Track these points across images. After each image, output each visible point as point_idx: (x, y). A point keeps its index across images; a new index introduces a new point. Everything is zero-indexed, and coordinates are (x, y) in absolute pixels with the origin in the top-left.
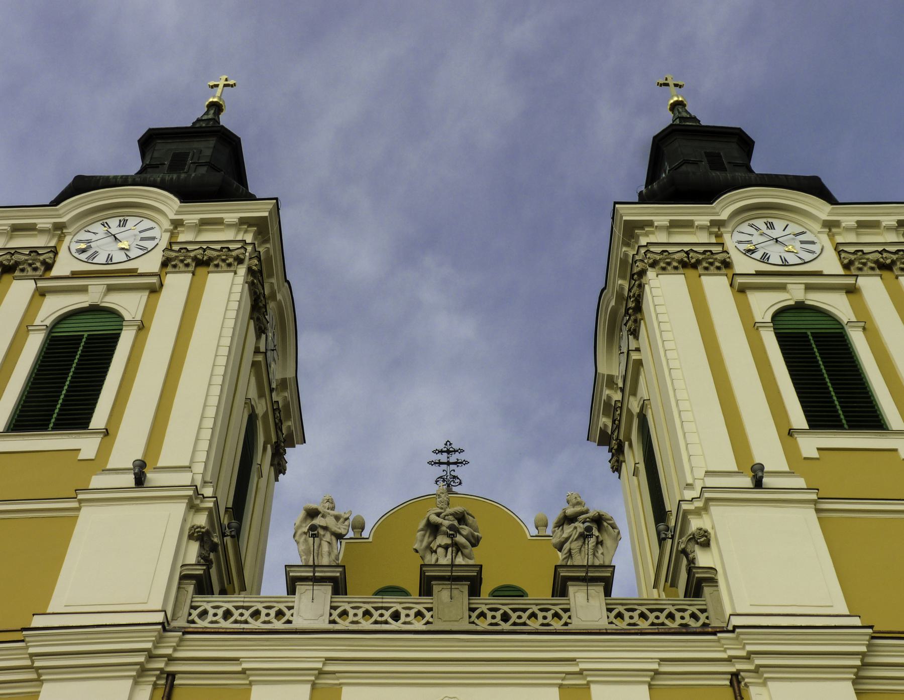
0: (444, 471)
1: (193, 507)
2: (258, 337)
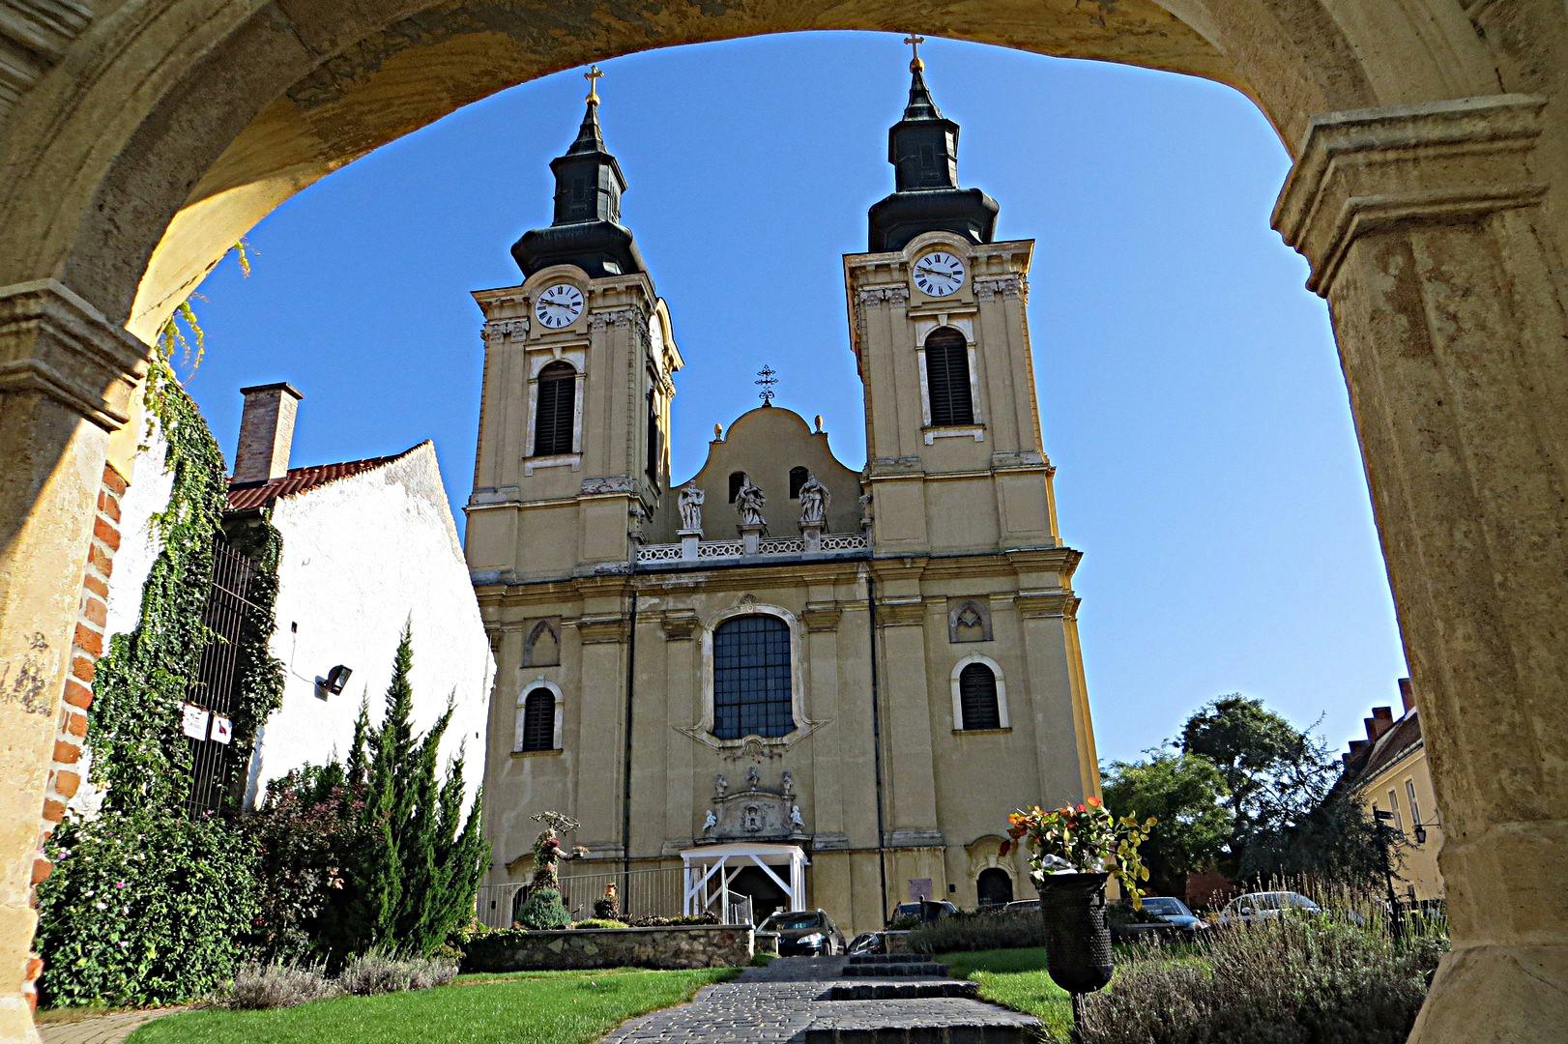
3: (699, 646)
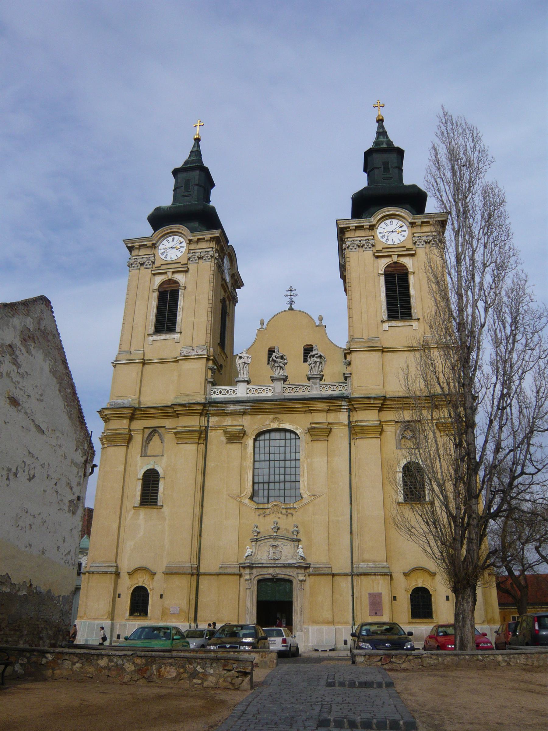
1: (208, 359)
3: (246, 446)
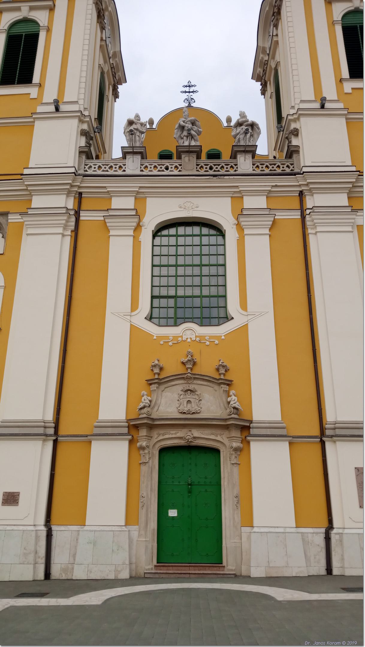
0: (187, 96)
1: (81, 121)
2: (102, 32)
